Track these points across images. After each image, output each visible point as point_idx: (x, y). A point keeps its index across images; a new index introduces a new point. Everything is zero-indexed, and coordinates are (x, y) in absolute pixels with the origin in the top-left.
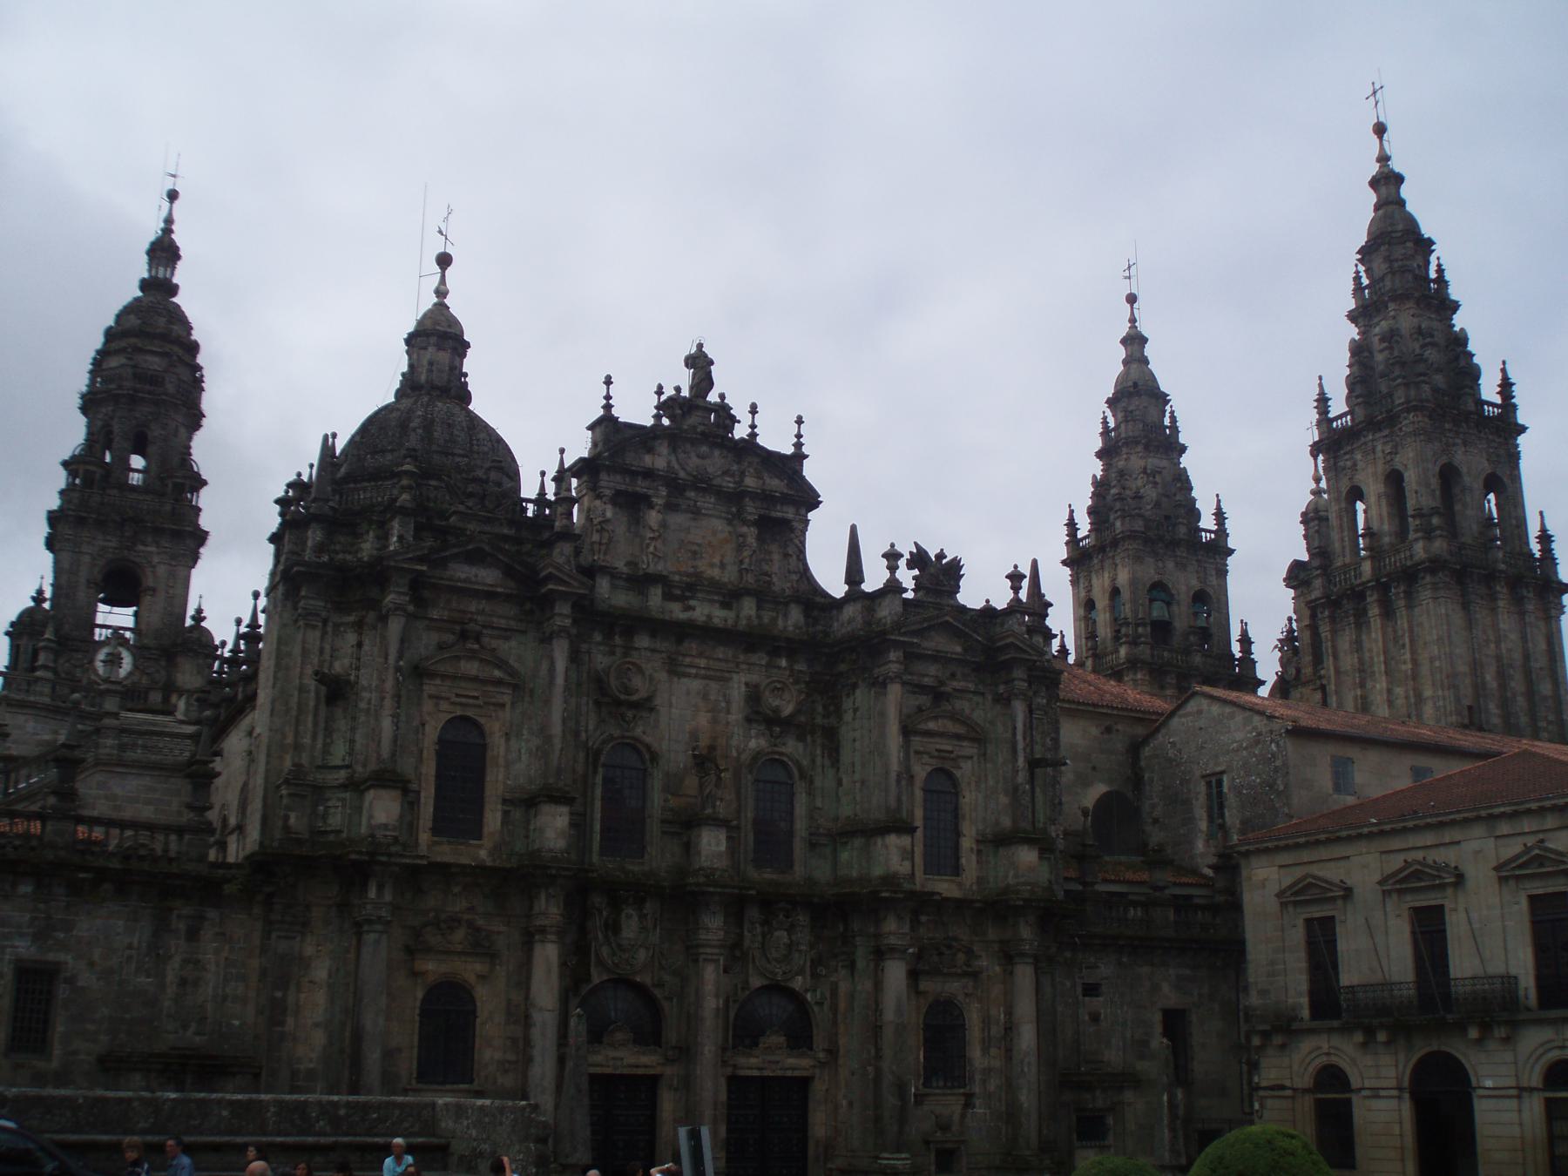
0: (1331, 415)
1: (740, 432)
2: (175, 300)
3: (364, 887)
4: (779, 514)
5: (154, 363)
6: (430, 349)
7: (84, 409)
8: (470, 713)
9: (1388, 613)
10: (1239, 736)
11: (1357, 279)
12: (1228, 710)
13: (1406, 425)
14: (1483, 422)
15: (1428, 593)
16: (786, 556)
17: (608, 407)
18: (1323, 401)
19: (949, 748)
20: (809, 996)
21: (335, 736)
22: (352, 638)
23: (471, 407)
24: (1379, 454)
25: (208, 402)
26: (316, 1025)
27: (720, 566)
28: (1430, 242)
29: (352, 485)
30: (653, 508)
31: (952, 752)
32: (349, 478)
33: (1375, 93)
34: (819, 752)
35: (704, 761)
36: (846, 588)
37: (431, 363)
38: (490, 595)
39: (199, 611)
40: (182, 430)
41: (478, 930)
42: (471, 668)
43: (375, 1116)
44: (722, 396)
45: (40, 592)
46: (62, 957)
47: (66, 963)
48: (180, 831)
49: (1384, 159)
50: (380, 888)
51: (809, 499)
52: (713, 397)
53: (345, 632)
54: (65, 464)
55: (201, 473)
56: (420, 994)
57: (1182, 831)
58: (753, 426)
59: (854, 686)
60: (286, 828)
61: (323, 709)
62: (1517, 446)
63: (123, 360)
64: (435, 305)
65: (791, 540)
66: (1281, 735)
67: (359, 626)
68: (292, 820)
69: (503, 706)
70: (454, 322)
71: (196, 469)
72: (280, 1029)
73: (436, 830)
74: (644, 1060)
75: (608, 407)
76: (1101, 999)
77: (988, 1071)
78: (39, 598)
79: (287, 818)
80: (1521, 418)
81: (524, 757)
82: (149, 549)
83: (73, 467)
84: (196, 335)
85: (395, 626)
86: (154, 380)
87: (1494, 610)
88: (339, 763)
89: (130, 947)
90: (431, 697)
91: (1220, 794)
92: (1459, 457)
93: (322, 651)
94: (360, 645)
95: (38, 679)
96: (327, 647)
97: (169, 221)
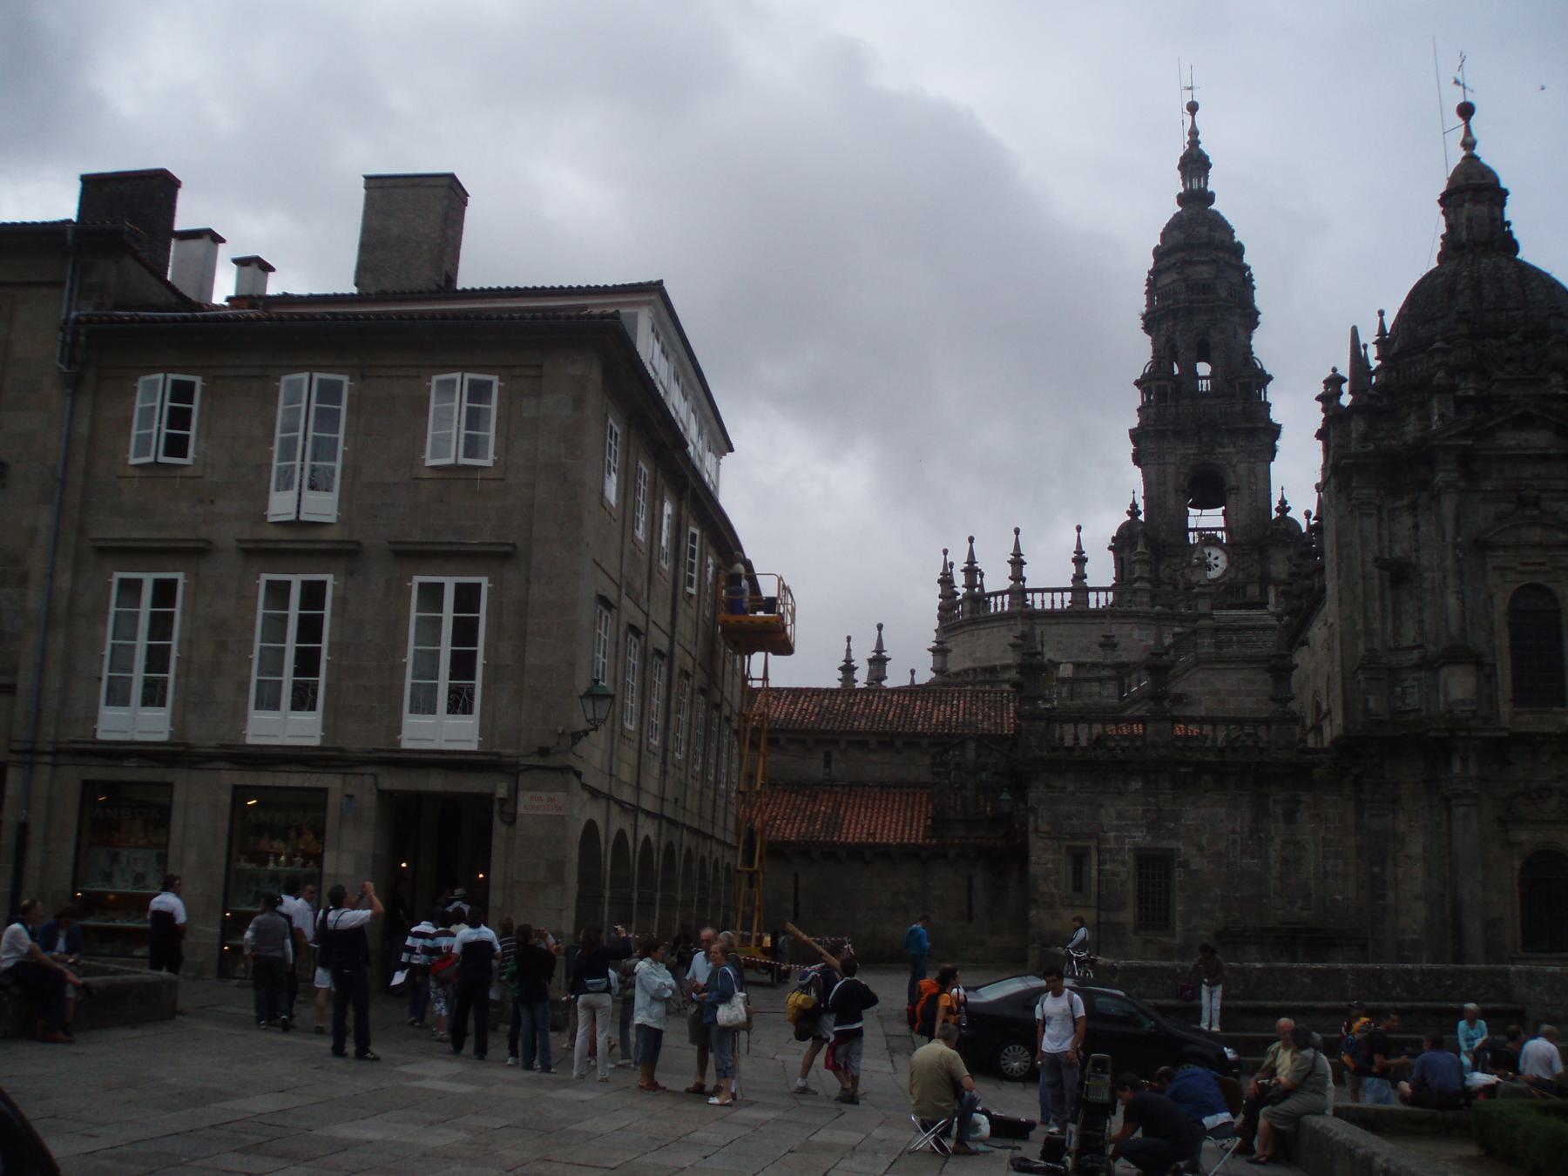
2: (1213, 207)
5: (1203, 272)
6: (1466, 205)
7: (1148, 328)
8: (1540, 580)
22: (1407, 521)
23: (1519, 256)
25: (1260, 300)
29: (1407, 360)
37: (1470, 220)
38: (1545, 458)
39: (1283, 502)
40: (1240, 331)
42: (1535, 534)
43: (1449, 982)
45: (1134, 506)
46: (1174, 844)
47: (1179, 850)
48: (1267, 722)
50: (1464, 761)
54: (1138, 383)
55: (1265, 368)
56: (1517, 864)
63: (1175, 276)
64: (1464, 158)
67: (1413, 508)
68: (1372, 703)
71: (1260, 367)
72: (1381, 902)
73: (1516, 701)
78: (1134, 511)
79: (1366, 701)
82: (1227, 450)
83: (1145, 385)
84: (1238, 237)
85: (1449, 504)
86: (1208, 288)
88: (1411, 643)
89: (1234, 832)
90: (1495, 568)
93: (1380, 537)
94: (1416, 527)
95: (1135, 592)
97: (1194, 133)
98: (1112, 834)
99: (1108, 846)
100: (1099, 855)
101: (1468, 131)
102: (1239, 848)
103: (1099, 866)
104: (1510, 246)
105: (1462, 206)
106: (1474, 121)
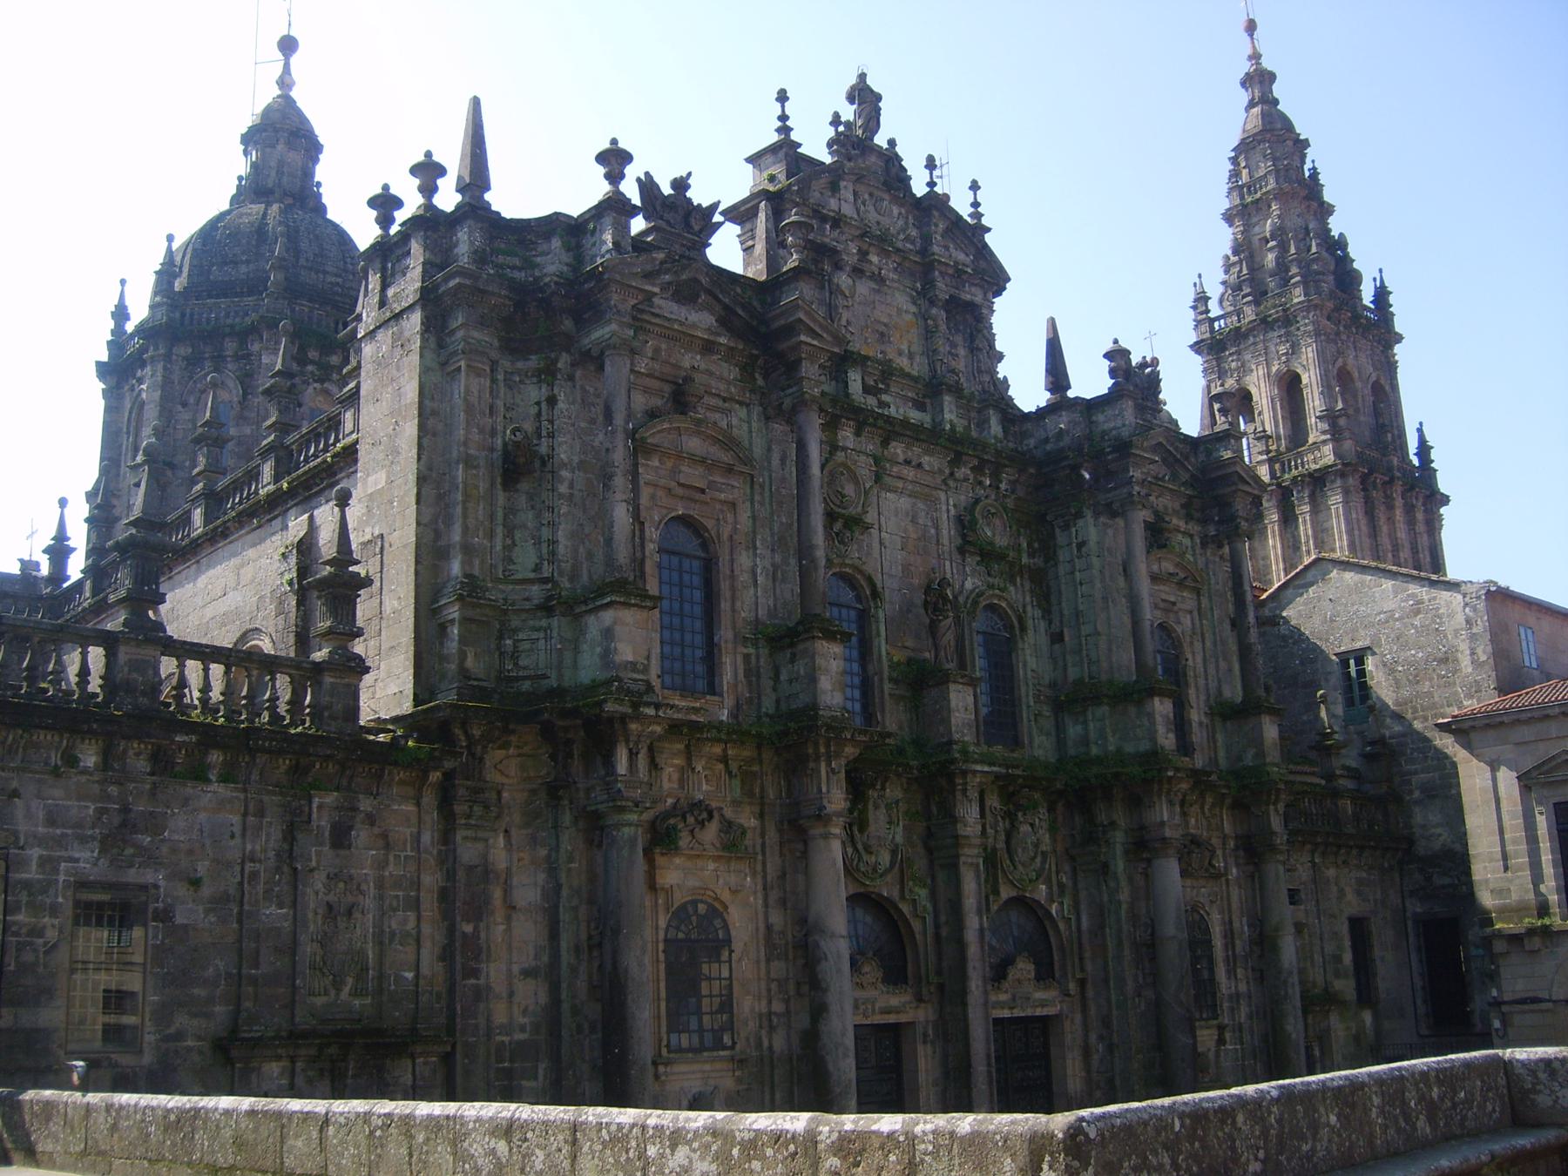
0: (1211, 315)
1: (919, 188)
3: (609, 763)
4: (968, 297)
6: (280, 147)
9: (1288, 519)
10: (1389, 605)
11: (1235, 174)
14: (1376, 325)
16: (973, 350)
17: (785, 130)
18: (1202, 299)
20: (1054, 909)
21: (518, 535)
22: (534, 392)
26: (527, 973)
27: (905, 353)
28: (1305, 144)
30: (841, 269)
34: (1028, 599)
35: (936, 598)
36: (1048, 395)
37: (281, 163)
41: (730, 824)
44: (892, 143)
46: (149, 876)
47: (156, 887)
49: (1255, 57)
50: (632, 755)
51: (994, 279)
52: (881, 140)
57: (1305, 718)
59: (1079, 515)
61: (501, 498)
62: (1394, 355)
65: (979, 331)
67: (547, 374)
70: (303, 120)
72: (473, 981)
74: (895, 1001)
75: (785, 130)
76: (1302, 907)
77: (1236, 997)
80: (1399, 326)
81: (760, 580)
85: (617, 370)
87: (1391, 520)
92: (1351, 361)
96: (500, 403)
98: (35, 853)
99: (25, 876)
100: (6, 892)
102: (261, 888)
103: (5, 916)
104: (321, 209)
106: (294, 60)
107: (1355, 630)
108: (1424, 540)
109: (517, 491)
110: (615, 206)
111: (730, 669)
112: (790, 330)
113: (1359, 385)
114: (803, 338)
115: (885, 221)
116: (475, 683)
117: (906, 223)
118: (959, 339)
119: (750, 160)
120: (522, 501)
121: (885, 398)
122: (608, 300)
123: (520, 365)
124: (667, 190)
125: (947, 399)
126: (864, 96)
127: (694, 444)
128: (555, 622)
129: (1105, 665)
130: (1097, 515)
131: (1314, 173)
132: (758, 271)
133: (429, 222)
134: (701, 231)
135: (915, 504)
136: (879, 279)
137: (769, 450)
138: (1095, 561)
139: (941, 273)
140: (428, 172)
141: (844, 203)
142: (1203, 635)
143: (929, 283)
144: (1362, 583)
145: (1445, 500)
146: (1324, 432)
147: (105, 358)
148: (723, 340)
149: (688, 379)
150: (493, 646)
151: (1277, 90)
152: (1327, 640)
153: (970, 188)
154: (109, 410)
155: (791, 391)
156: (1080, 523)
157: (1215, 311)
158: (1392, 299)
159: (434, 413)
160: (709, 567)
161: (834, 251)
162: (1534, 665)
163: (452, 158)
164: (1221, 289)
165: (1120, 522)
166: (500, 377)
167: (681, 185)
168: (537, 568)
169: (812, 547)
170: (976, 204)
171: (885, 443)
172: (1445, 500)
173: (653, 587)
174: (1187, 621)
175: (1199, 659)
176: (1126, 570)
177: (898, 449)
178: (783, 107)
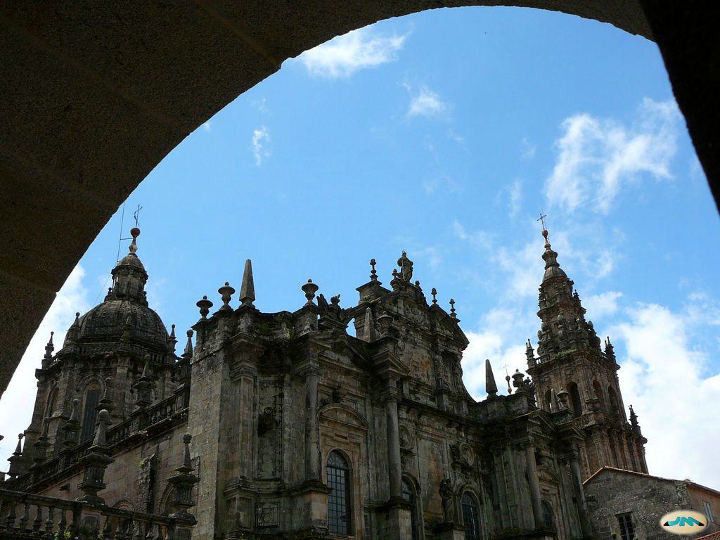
1: (430, 303)
4: (451, 351)
8: (342, 448)
12: (629, 478)
13: (578, 362)
15: (599, 439)
17: (374, 277)
18: (530, 351)
19: (547, 488)
21: (265, 458)
22: (272, 391)
24: (564, 375)
27: (425, 375)
28: (572, 283)
31: (548, 491)
32: (83, 339)
33: (542, 218)
37: (129, 283)
44: (417, 283)
49: (548, 246)
52: (412, 281)
53: (267, 387)
58: (435, 301)
59: (504, 449)
60: (238, 522)
61: (257, 439)
66: (683, 488)
67: (279, 383)
68: (242, 518)
69: (359, 445)
75: (374, 277)
79: (238, 516)
87: (622, 449)
91: (630, 524)
92: (598, 378)
101: (134, 241)
105: (127, 276)
107: (624, 503)
108: (637, 460)
109: (265, 437)
110: (308, 309)
111: (359, 522)
112: (385, 365)
113: (602, 388)
114: (391, 369)
115: (416, 317)
116: (245, 529)
117: (425, 318)
118: (447, 369)
119: (357, 289)
120: (267, 442)
121: (417, 395)
122: (308, 351)
123: (266, 379)
124: (329, 303)
125: (445, 397)
126: (405, 263)
127: (343, 417)
128: (282, 500)
129: (520, 520)
130: (513, 449)
131: (576, 295)
132: (366, 338)
133: (226, 312)
134: (344, 320)
135: (432, 445)
136: (415, 344)
137: (374, 419)
138: (513, 471)
139: (440, 340)
140: (226, 292)
141: (400, 309)
142: (561, 506)
143: (435, 345)
144: (626, 480)
145: (645, 441)
146: (589, 410)
147: (40, 367)
148: (354, 369)
149: (339, 387)
150: (253, 511)
151: (558, 260)
152: (611, 508)
153: (450, 303)
154: (39, 392)
155: (384, 392)
156: (505, 453)
157: (536, 356)
158: (614, 350)
159: (228, 400)
160: (348, 474)
161: (396, 330)
162: (713, 521)
163: (237, 285)
164: (538, 346)
165: (523, 453)
166: (258, 384)
167: (335, 300)
168: (274, 474)
169: (395, 465)
170: (453, 310)
171: (419, 416)
172: (645, 441)
173: (325, 482)
174: (554, 499)
175: (561, 518)
176: (527, 476)
177: (424, 419)
178: (373, 267)
